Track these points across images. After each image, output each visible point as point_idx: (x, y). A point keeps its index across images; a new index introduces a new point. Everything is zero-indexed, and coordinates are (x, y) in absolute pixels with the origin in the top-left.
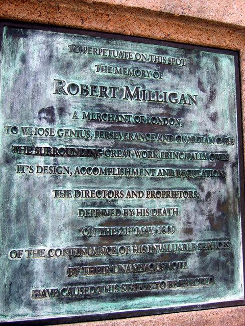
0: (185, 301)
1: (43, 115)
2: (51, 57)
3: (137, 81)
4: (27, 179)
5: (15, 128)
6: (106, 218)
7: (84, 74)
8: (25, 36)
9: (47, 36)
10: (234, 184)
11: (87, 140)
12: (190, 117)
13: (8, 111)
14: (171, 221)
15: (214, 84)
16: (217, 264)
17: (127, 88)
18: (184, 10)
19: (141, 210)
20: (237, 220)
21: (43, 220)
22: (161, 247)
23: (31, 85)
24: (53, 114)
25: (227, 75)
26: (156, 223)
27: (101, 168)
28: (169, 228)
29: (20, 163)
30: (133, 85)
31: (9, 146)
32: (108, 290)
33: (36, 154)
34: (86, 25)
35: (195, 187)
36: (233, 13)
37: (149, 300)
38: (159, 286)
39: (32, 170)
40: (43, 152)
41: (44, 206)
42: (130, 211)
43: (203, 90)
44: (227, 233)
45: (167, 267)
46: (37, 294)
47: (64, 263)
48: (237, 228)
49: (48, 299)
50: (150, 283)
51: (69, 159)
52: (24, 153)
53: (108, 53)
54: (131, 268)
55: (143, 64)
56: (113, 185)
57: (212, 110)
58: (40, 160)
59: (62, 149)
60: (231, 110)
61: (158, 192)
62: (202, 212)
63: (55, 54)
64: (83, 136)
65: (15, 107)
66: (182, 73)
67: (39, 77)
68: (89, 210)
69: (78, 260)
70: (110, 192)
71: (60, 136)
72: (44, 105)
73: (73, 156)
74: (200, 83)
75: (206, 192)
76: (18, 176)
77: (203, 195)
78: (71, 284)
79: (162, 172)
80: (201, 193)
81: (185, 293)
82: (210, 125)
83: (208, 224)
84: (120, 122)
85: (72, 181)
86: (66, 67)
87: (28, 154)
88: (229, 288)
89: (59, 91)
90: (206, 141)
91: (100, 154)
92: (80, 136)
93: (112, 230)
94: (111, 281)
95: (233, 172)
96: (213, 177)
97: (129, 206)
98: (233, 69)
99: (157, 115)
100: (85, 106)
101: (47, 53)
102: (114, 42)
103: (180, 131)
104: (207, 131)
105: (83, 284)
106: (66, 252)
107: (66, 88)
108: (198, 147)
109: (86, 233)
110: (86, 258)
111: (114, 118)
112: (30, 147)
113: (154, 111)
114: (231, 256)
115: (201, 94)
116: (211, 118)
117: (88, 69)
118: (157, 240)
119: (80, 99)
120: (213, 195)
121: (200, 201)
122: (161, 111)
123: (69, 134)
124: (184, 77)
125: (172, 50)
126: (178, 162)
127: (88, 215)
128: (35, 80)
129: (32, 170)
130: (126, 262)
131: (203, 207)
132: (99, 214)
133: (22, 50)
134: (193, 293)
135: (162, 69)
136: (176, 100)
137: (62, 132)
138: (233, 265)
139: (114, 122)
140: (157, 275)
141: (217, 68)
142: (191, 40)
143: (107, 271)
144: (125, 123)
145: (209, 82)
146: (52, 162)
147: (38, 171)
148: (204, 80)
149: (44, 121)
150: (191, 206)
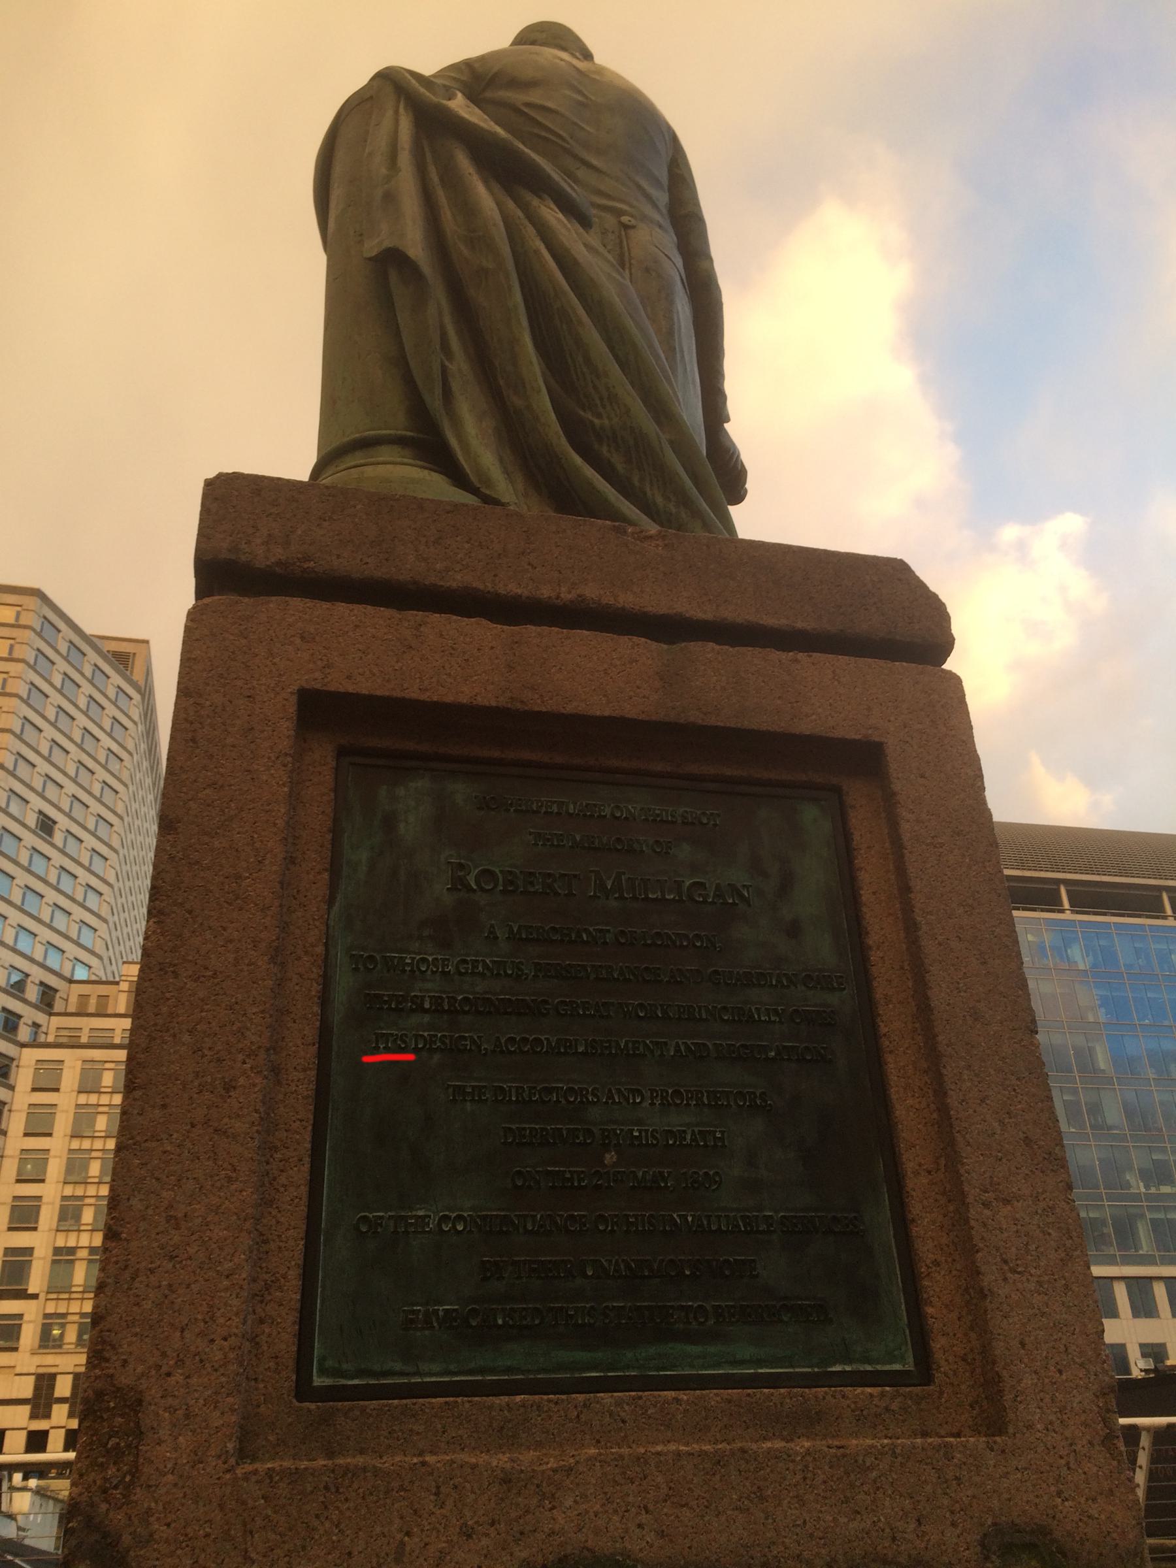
0: (760, 1363)
5: (371, 958)
18: (705, 714)
19: (640, 1131)
22: (690, 1219)
27: (547, 1039)
28: (706, 1173)
29: (382, 1029)
32: (571, 1316)
33: (412, 1010)
36: (813, 714)
38: (691, 1316)
39: (405, 1042)
40: (427, 1006)
42: (616, 1134)
50: (672, 1307)
52: (390, 1009)
54: (622, 1267)
61: (677, 1093)
64: (510, 972)
68: (524, 1129)
71: (460, 974)
73: (490, 1013)
79: (682, 1048)
89: (459, 884)
91: (546, 1009)
92: (502, 972)
93: (575, 1176)
106: (476, 1222)
111: (573, 936)
112: (401, 995)
123: (480, 969)
129: (405, 1042)
137: (465, 966)
147: (416, 1044)
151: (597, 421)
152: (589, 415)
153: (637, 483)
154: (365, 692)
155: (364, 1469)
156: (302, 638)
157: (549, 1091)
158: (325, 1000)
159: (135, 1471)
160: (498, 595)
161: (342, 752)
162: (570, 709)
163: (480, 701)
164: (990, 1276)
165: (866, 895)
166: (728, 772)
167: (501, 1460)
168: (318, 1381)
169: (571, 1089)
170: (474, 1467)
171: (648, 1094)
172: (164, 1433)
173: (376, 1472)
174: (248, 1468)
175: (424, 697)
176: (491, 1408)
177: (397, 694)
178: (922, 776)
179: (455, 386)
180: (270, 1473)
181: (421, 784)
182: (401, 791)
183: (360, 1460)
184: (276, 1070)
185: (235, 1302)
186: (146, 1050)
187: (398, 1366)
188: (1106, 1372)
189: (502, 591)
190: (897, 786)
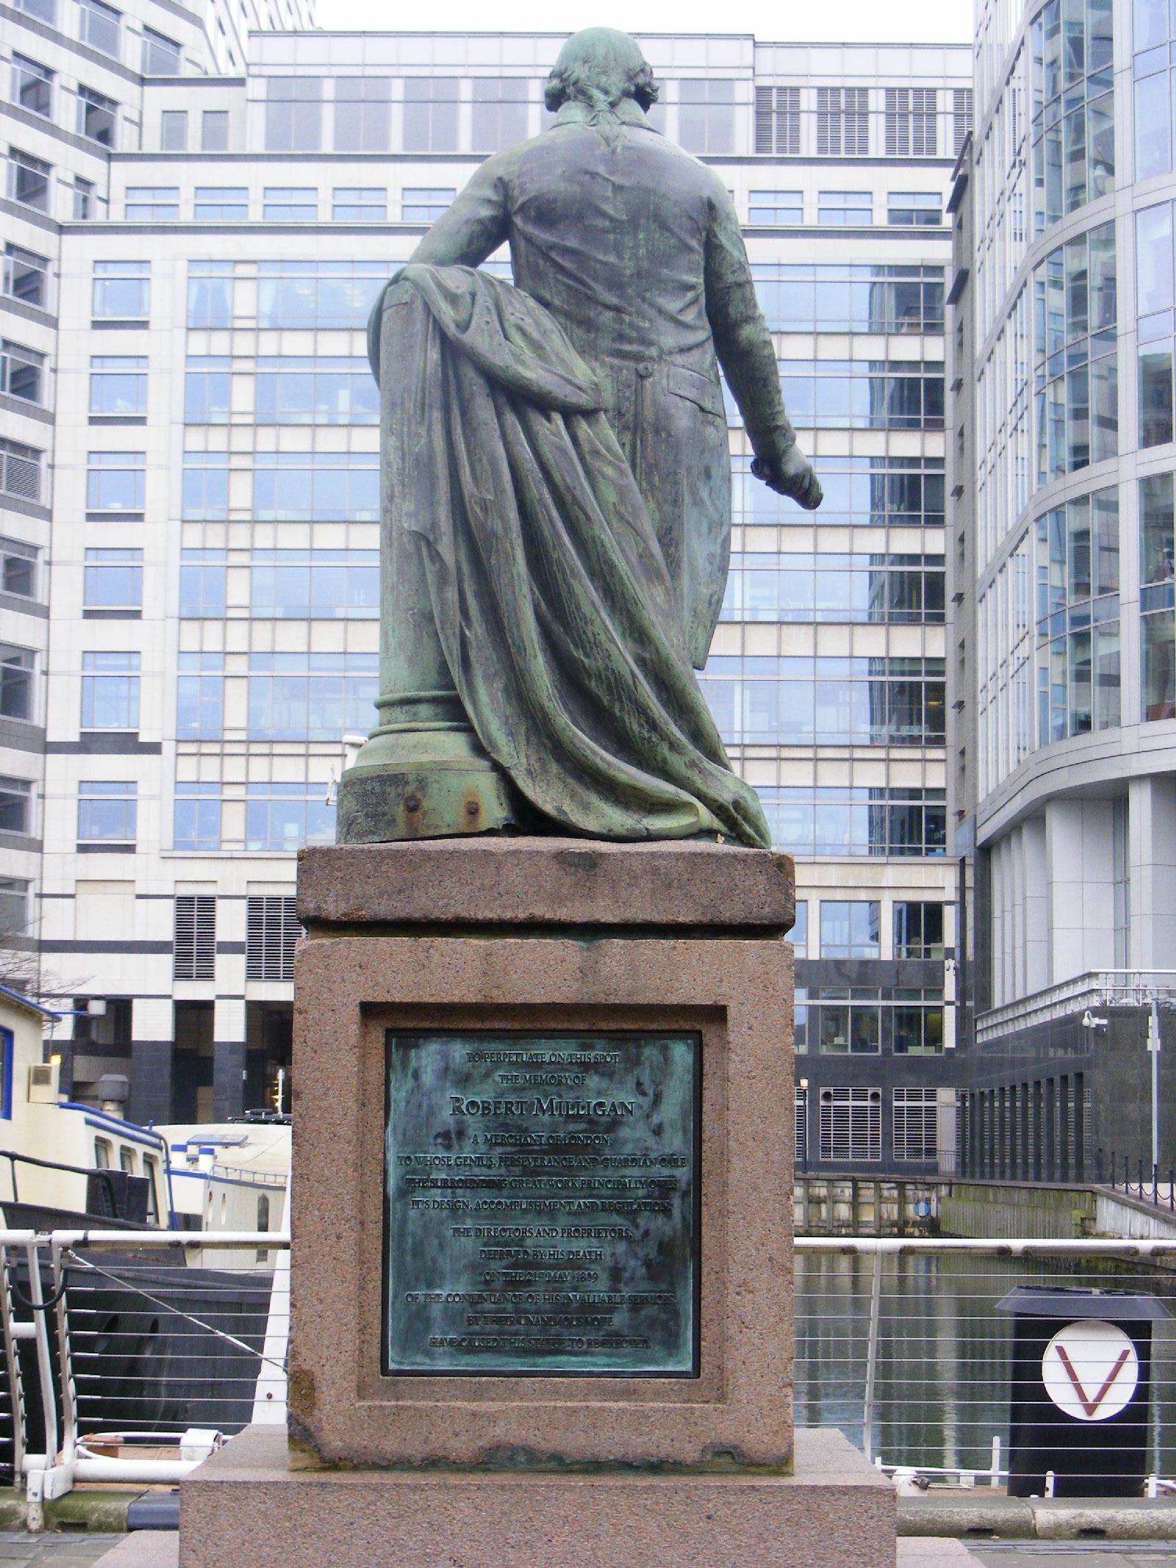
0: (609, 1365)
1: (440, 1140)
2: (447, 1069)
3: (552, 1089)
4: (423, 1215)
5: (409, 1158)
6: (511, 1260)
7: (485, 1087)
8: (417, 1046)
9: (442, 1044)
10: (684, 1218)
11: (489, 1167)
12: (625, 1132)
13: (400, 1137)
14: (592, 1266)
15: (660, 1083)
16: (653, 1322)
17: (539, 1101)
20: (686, 1267)
21: (440, 1259)
23: (425, 1105)
24: (450, 1139)
25: (680, 1069)
26: (572, 1268)
30: (546, 1096)
31: (403, 1177)
35: (626, 1223)
37: (564, 1358)
41: (441, 1246)
43: (644, 1094)
44: (672, 1284)
45: (587, 1323)
46: (434, 1343)
47: (464, 1309)
48: (686, 1278)
49: (447, 1348)
51: (468, 1191)
53: (514, 1058)
55: (560, 1067)
56: (520, 1221)
57: (655, 1119)
58: (436, 1194)
59: (460, 1180)
60: (684, 1115)
61: (577, 1230)
62: (635, 1256)
63: (452, 1066)
65: (408, 1133)
66: (613, 1072)
67: (433, 1095)
69: (479, 1306)
70: (517, 1229)
72: (438, 1128)
74: (639, 1084)
75: (642, 1231)
76: (413, 1213)
77: (638, 1234)
78: (472, 1334)
80: (635, 1231)
81: (609, 1355)
82: (651, 1141)
83: (644, 1270)
84: (530, 1144)
85: (472, 1217)
86: (464, 1080)
87: (423, 1187)
88: (670, 1355)
89: (457, 1110)
90: (645, 1163)
94: (516, 1334)
95: (683, 1203)
96: (653, 1211)
97: (540, 1246)
98: (689, 1058)
99: (578, 1132)
100: (487, 1127)
101: (442, 1065)
102: (522, 1042)
103: (608, 1152)
104: (647, 1149)
105: (484, 1334)
107: (464, 1107)
108: (635, 1172)
109: (488, 1278)
110: (488, 1306)
113: (572, 1127)
114: (675, 1314)
115: (641, 1099)
116: (654, 1132)
117: (490, 1081)
118: (574, 1289)
119: (481, 1119)
120: (652, 1233)
121: (634, 1241)
122: (583, 1126)
124: (616, 1077)
125: (601, 1043)
126: (604, 1192)
127: (490, 1256)
128: (430, 1099)
130: (535, 1313)
131: (638, 1249)
132: (501, 1256)
133: (413, 1064)
134: (618, 1356)
135: (586, 1071)
136: (604, 1111)
138: (678, 1325)
139: (521, 1145)
140: (573, 1330)
141: (666, 1060)
143: (512, 1322)
144: (536, 1145)
146: (450, 1195)
148: (646, 1080)
149: (440, 1148)
150: (621, 1247)
151: (586, 660)
152: (578, 654)
153: (618, 714)
154: (397, 1000)
155: (410, 1407)
156: (360, 967)
157: (504, 1230)
159: (314, 1404)
160: (478, 920)
161: (389, 1033)
162: (520, 1000)
164: (733, 1330)
166: (625, 1026)
167: (473, 1406)
168: (392, 1366)
169: (517, 1229)
170: (459, 1409)
171: (560, 1231)
172: (324, 1389)
173: (416, 1409)
174: (361, 1404)
175: (432, 1000)
176: (471, 1382)
177: (416, 1000)
178: (750, 1028)
179: (473, 655)
180: (369, 1407)
183: (409, 1403)
184: (362, 1223)
185: (350, 1336)
186: (299, 1219)
187: (428, 1361)
188: (788, 1377)
189: (480, 917)
190: (731, 1038)
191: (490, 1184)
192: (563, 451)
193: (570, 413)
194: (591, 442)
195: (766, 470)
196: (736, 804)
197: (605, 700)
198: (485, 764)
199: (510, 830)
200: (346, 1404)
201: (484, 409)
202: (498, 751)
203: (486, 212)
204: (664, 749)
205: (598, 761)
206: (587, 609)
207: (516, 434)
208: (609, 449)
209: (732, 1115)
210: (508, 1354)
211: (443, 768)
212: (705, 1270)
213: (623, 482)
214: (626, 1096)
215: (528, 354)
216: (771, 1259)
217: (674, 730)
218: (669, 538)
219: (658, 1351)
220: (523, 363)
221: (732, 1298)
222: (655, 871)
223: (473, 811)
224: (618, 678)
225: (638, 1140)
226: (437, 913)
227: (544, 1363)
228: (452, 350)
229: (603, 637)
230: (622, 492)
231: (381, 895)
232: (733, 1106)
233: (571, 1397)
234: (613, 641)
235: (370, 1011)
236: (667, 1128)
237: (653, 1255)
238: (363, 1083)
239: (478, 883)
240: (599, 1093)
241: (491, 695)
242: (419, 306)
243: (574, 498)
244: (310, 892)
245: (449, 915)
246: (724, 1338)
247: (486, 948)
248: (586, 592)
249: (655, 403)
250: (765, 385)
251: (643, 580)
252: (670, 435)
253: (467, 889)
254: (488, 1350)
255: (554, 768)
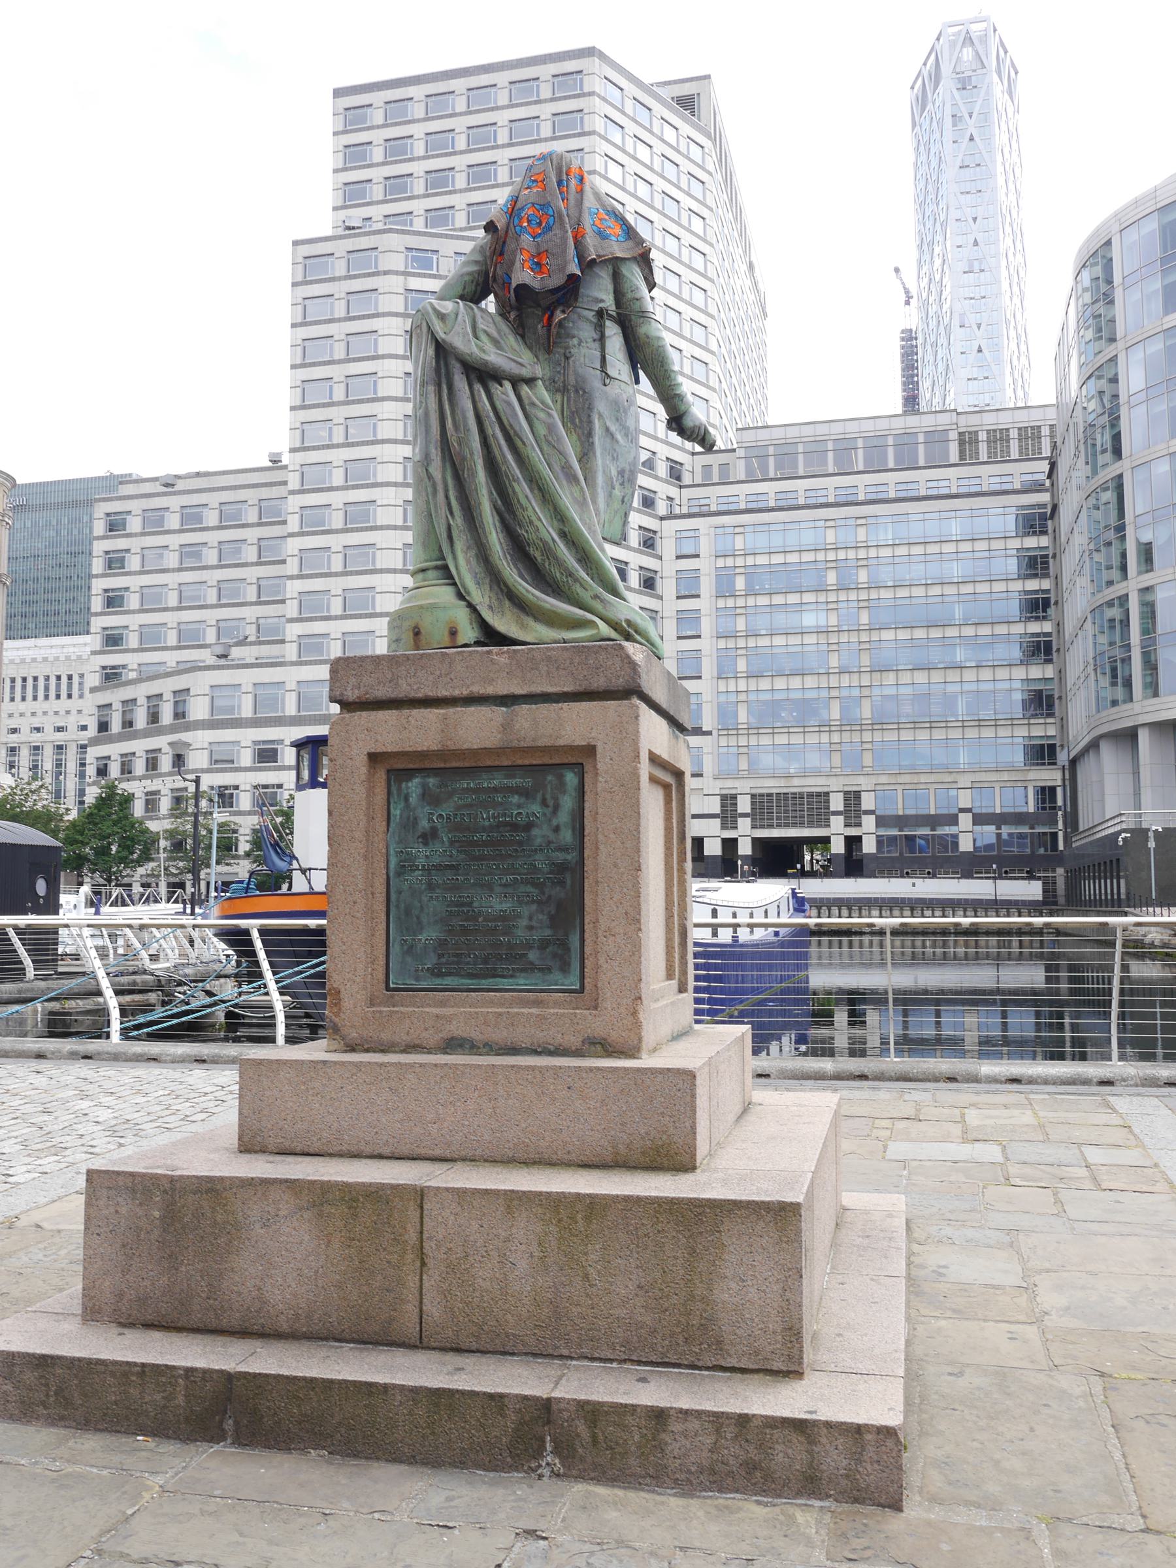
12: (535, 832)
34: (448, 765)
37: (498, 980)
43: (547, 806)
57: (555, 822)
60: (573, 820)
62: (542, 912)
82: (552, 836)
89: (430, 820)
142: (534, 762)
145: (553, 798)
158: (388, 868)
161: (388, 771)
163: (432, 748)
164: (602, 961)
165: (586, 813)
168: (392, 986)
179: (455, 534)
181: (416, 781)
182: (410, 784)
183: (402, 1009)
184: (372, 894)
190: (599, 765)
191: (451, 867)
192: (509, 404)
193: (516, 381)
194: (529, 398)
195: (674, 425)
196: (628, 622)
197: (539, 559)
198: (463, 603)
199: (478, 643)
200: (359, 1009)
201: (460, 382)
202: (469, 593)
203: (475, 268)
204: (579, 590)
205: (531, 597)
206: (523, 501)
207: (480, 395)
208: (543, 403)
209: (600, 817)
210: (462, 976)
211: (433, 607)
212: (586, 921)
213: (550, 421)
214: (536, 808)
215: (489, 346)
216: (626, 913)
217: (583, 574)
218: (585, 456)
219: (557, 975)
220: (484, 351)
221: (601, 939)
222: (549, 659)
223: (453, 633)
224: (545, 543)
225: (544, 836)
226: (413, 695)
227: (485, 983)
228: (442, 350)
229: (534, 518)
230: (551, 428)
231: (379, 683)
232: (600, 811)
233: (502, 1005)
234: (540, 520)
235: (374, 758)
236: (562, 828)
237: (553, 912)
238: (370, 804)
239: (438, 673)
240: (519, 806)
241: (468, 562)
242: (424, 324)
243: (515, 432)
244: (338, 684)
245: (420, 695)
246: (597, 967)
247: (444, 714)
248: (522, 490)
249: (576, 374)
250: (662, 366)
251: (565, 482)
252: (585, 392)
253: (431, 678)
254: (450, 974)
255: (507, 603)
